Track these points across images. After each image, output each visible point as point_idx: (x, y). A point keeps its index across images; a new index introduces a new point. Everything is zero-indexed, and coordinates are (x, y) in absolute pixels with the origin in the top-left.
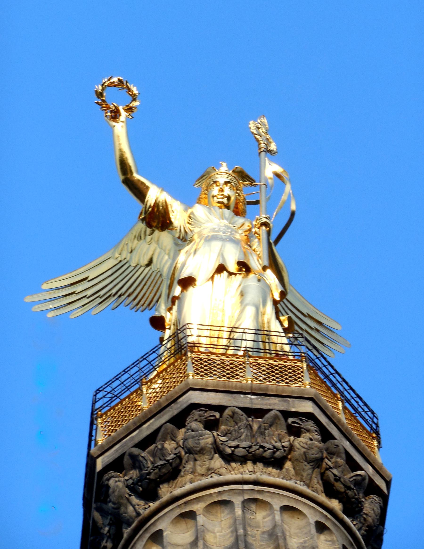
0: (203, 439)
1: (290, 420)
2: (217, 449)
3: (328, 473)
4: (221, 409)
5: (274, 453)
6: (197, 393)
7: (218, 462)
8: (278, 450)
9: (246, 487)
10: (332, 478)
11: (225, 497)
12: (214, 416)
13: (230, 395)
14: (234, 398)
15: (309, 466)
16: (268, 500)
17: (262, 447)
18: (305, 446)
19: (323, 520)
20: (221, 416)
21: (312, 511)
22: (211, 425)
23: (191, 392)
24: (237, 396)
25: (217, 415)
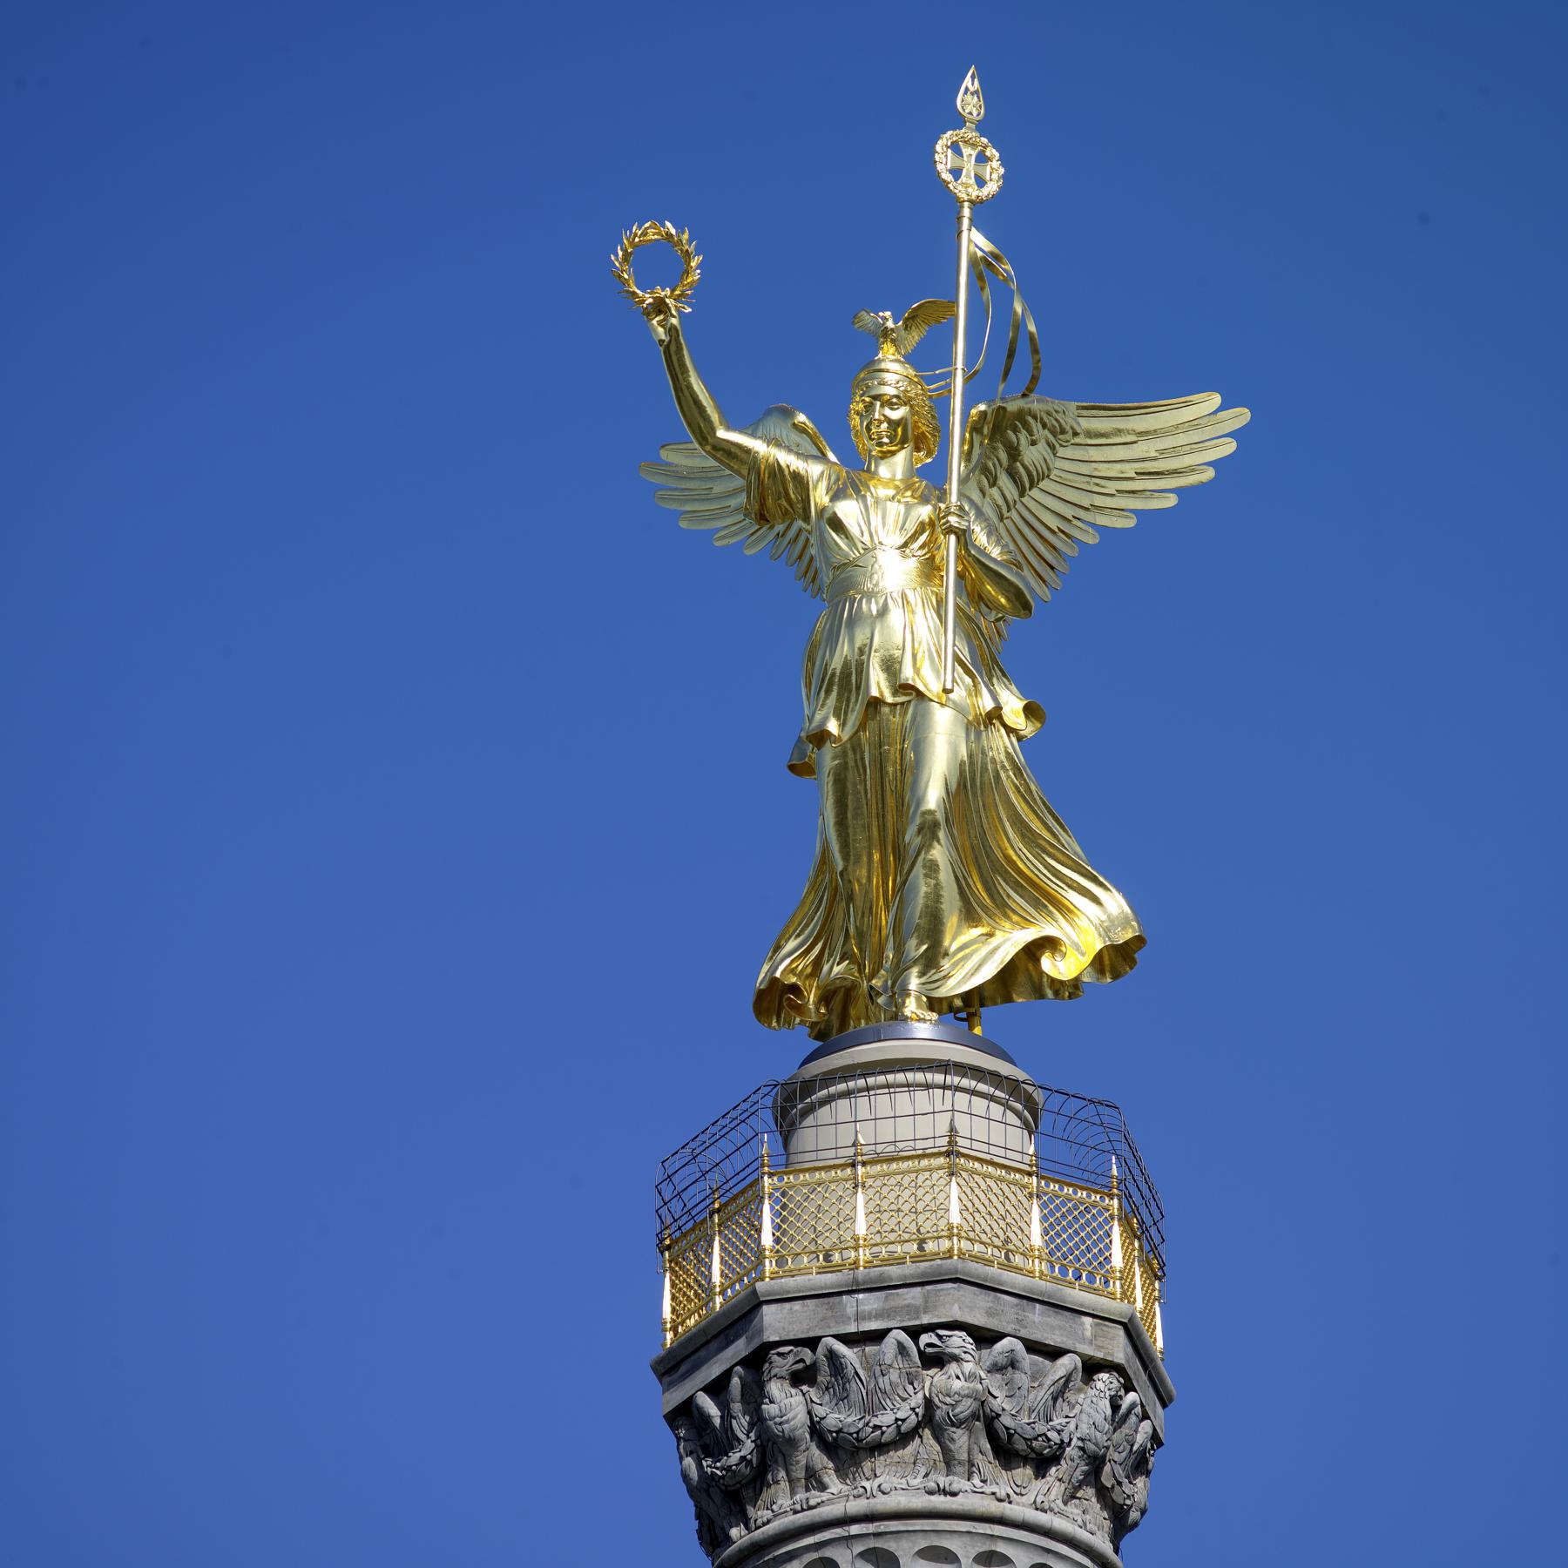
0: (787, 1422)
1: (925, 1339)
2: (816, 1430)
3: (997, 1425)
4: (812, 1343)
5: (899, 1427)
6: (773, 1307)
7: (818, 1457)
8: (903, 1421)
9: (855, 1529)
10: (1004, 1436)
11: (828, 1553)
12: (802, 1360)
13: (826, 1300)
14: (832, 1308)
15: (959, 1431)
16: (890, 1545)
17: (876, 1427)
18: (948, 1400)
19: (987, 1546)
20: (814, 1350)
21: (966, 1539)
22: (801, 1377)
23: (765, 1308)
24: (836, 1299)
25: (807, 1354)
